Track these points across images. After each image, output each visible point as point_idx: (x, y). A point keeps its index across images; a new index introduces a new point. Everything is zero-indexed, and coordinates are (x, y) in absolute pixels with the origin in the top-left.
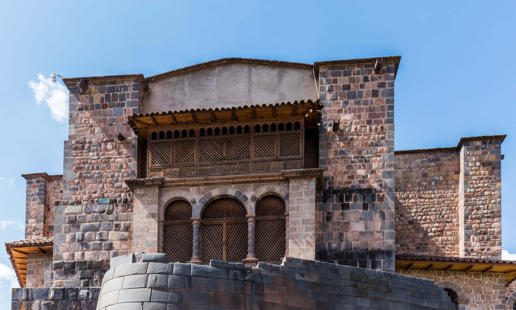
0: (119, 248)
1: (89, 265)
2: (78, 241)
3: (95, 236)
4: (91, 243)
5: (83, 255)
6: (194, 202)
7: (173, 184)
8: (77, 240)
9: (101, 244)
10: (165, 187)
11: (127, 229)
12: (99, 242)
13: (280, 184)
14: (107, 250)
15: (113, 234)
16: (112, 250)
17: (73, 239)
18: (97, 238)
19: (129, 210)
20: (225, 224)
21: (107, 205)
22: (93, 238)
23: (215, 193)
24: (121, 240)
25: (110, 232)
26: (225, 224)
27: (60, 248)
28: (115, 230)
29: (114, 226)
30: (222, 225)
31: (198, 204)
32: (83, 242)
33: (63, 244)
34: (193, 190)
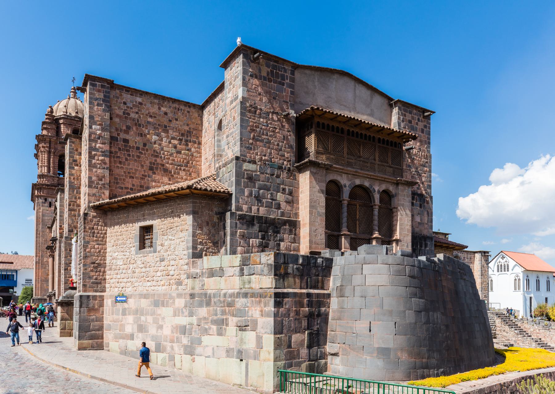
0: (285, 209)
1: (265, 220)
2: (254, 197)
3: (268, 195)
4: (264, 201)
5: (258, 209)
6: (345, 186)
7: (335, 169)
8: (254, 196)
9: (272, 202)
10: (330, 170)
11: (291, 193)
12: (270, 200)
13: (392, 185)
14: (277, 209)
15: (280, 196)
16: (279, 209)
17: (251, 194)
18: (269, 197)
19: (292, 178)
20: (358, 205)
21: (276, 170)
22: (266, 197)
23: (358, 182)
24: (286, 202)
25: (278, 194)
26: (358, 205)
27: (240, 200)
28: (282, 193)
29: (281, 189)
30: (356, 205)
31: (347, 188)
32: (258, 199)
33: (243, 197)
34: (344, 176)
